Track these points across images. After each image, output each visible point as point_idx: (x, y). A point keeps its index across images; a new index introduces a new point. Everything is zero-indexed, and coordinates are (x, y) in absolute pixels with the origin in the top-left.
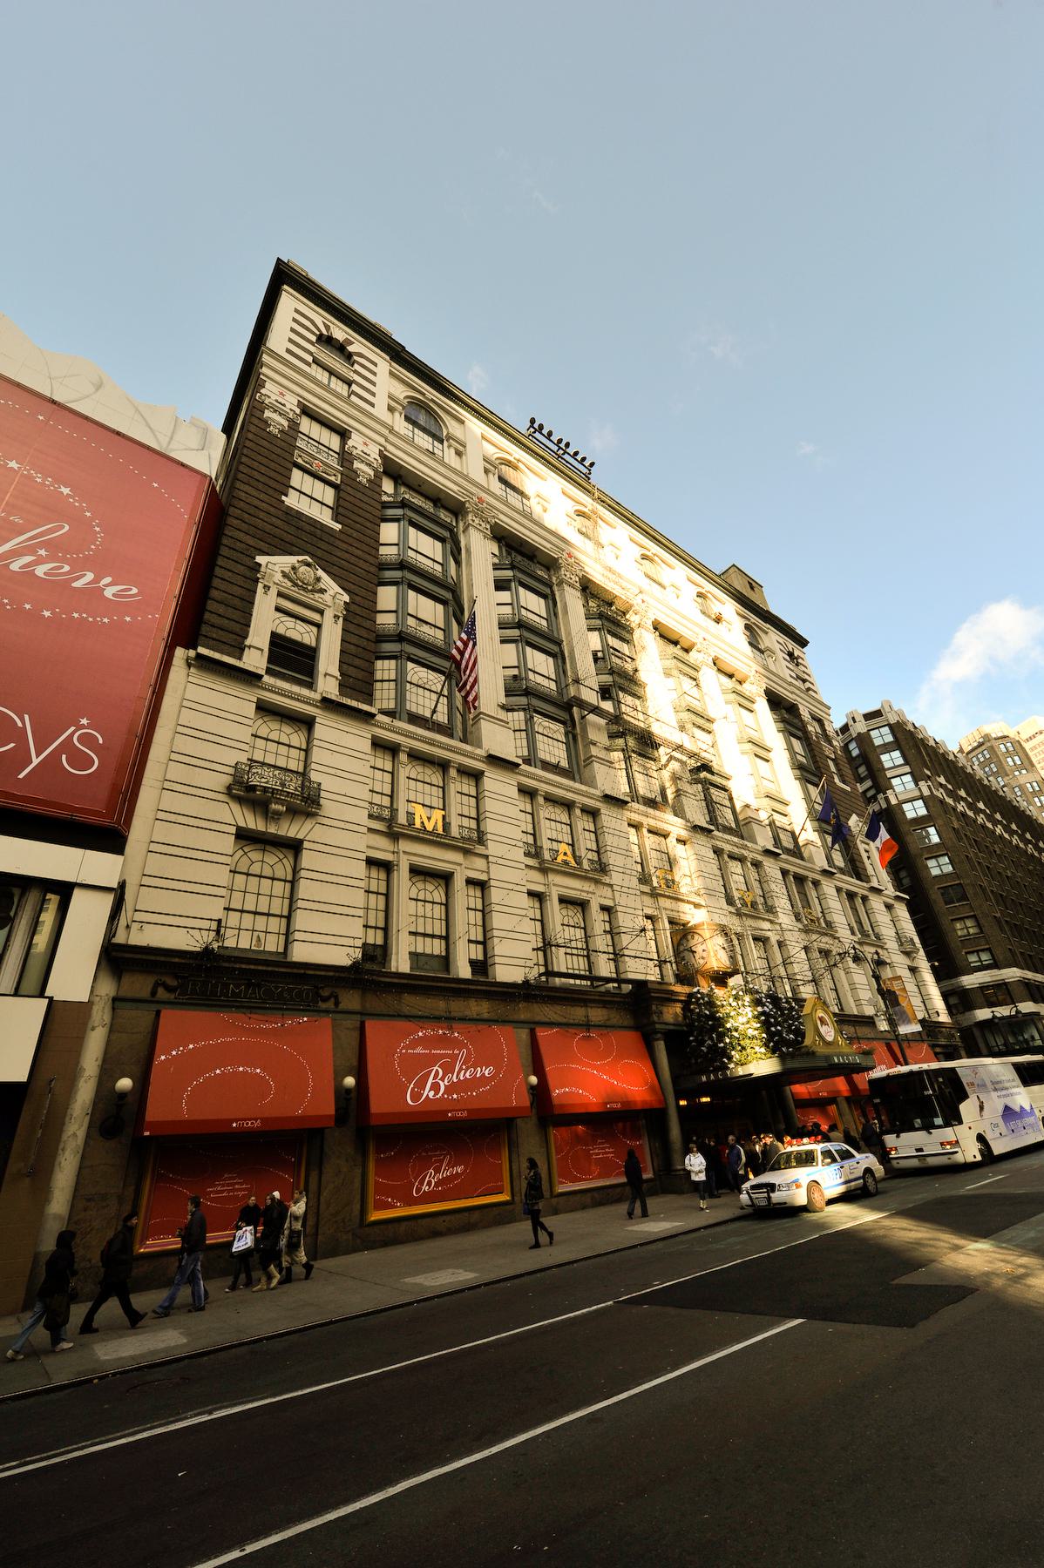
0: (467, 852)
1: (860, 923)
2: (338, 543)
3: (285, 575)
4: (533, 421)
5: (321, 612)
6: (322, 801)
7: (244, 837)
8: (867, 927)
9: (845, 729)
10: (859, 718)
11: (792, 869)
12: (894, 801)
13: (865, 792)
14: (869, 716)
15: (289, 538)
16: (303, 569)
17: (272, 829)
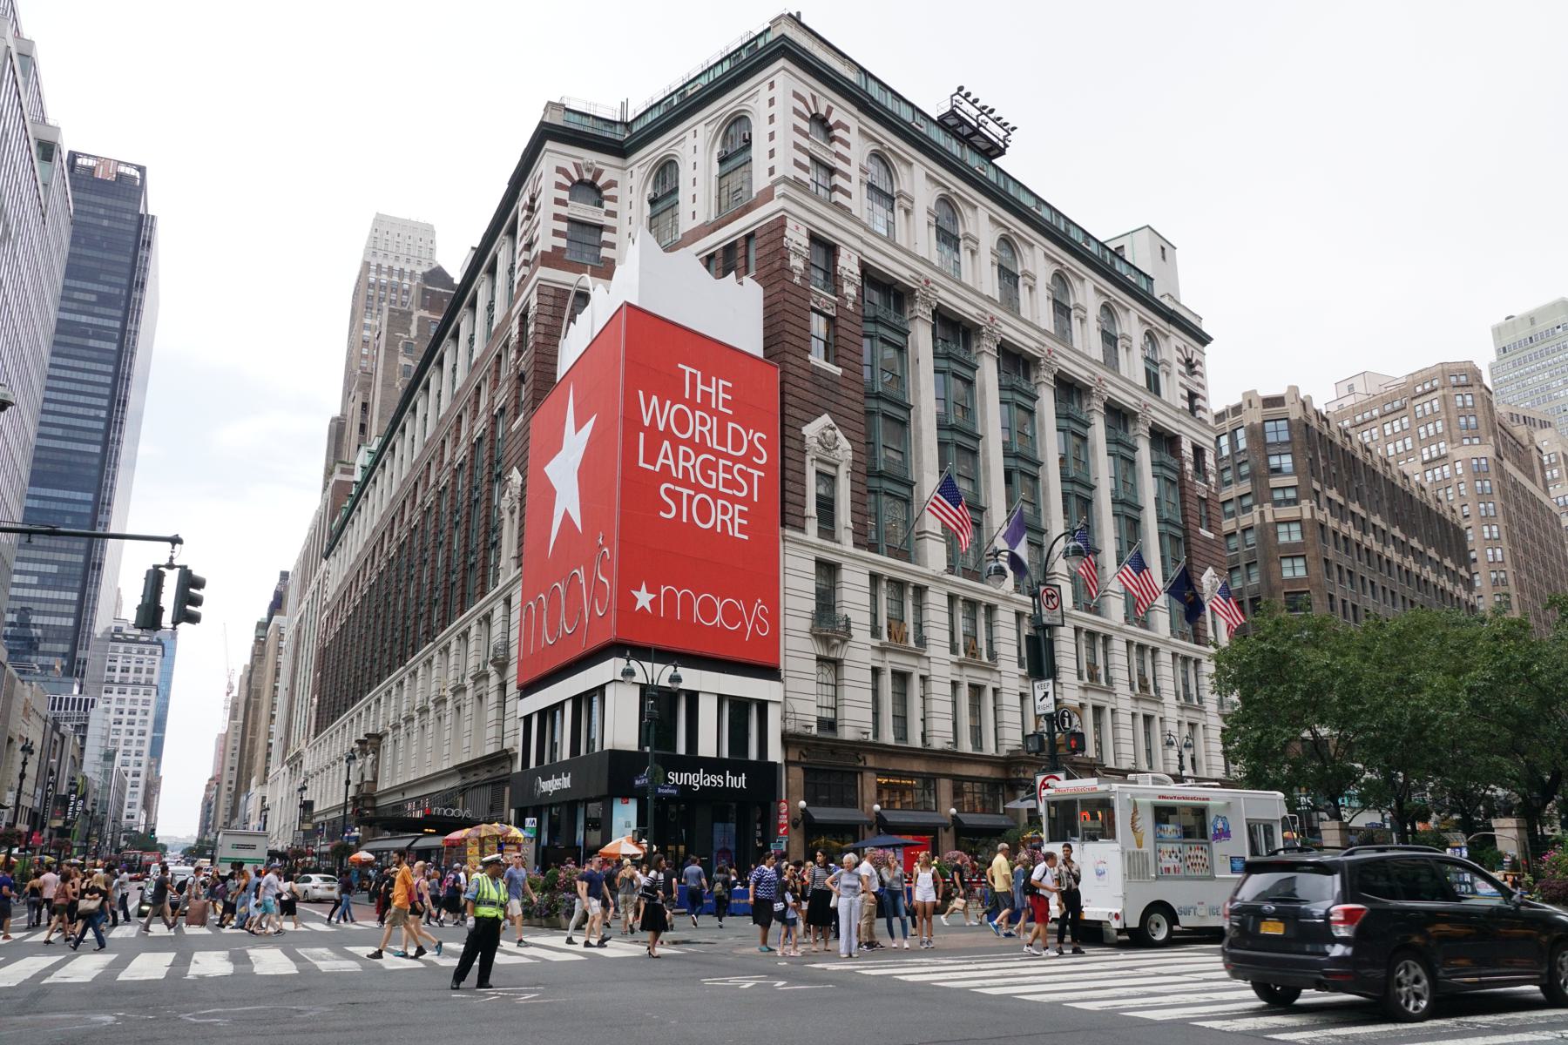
0: (919, 656)
1: (1186, 687)
2: (843, 391)
3: (819, 442)
4: (961, 89)
5: (836, 466)
6: (853, 631)
7: (820, 659)
8: (1193, 691)
9: (1237, 410)
10: (1257, 404)
11: (1136, 640)
12: (1269, 519)
13: (1241, 497)
14: (1270, 402)
15: (815, 399)
16: (829, 432)
17: (832, 655)
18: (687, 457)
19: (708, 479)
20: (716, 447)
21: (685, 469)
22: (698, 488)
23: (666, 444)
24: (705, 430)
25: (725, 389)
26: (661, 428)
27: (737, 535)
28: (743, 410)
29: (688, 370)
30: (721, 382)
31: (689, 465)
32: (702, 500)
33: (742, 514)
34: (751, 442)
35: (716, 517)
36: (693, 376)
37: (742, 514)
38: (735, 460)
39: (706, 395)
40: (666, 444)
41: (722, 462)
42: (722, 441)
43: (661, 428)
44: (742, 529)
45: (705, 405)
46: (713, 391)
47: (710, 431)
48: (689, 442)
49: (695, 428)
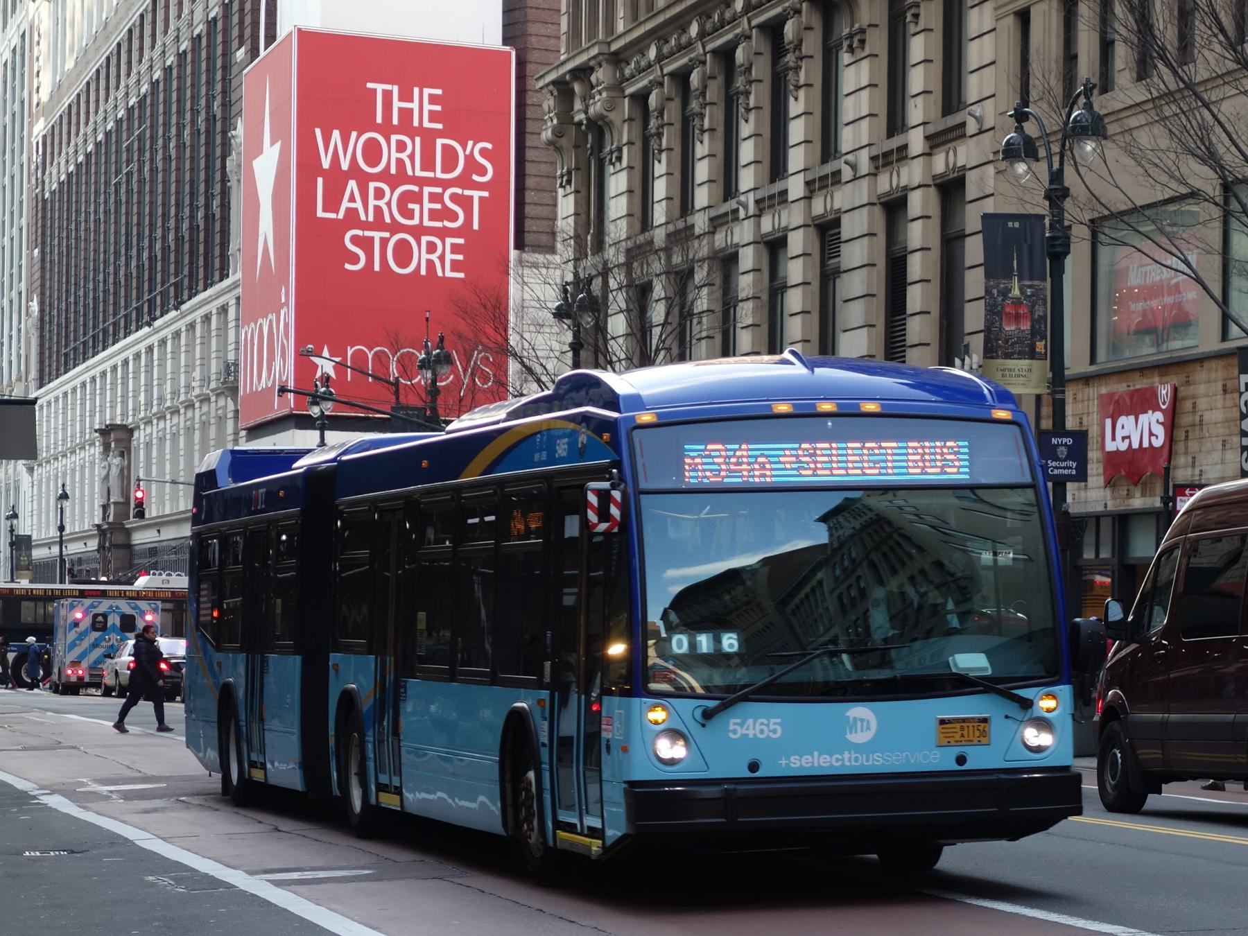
18: (379, 194)
19: (409, 214)
20: (419, 173)
21: (378, 210)
22: (395, 227)
23: (352, 185)
24: (404, 156)
25: (433, 99)
26: (345, 166)
27: (449, 274)
28: (457, 121)
29: (380, 88)
30: (427, 91)
31: (382, 203)
32: (402, 244)
33: (455, 249)
34: (470, 158)
35: (420, 257)
36: (387, 95)
37: (455, 249)
38: (445, 184)
39: (406, 114)
40: (352, 185)
41: (427, 190)
42: (428, 164)
43: (345, 166)
44: (455, 266)
45: (406, 123)
46: (415, 106)
47: (412, 157)
48: (384, 176)
49: (390, 156)
